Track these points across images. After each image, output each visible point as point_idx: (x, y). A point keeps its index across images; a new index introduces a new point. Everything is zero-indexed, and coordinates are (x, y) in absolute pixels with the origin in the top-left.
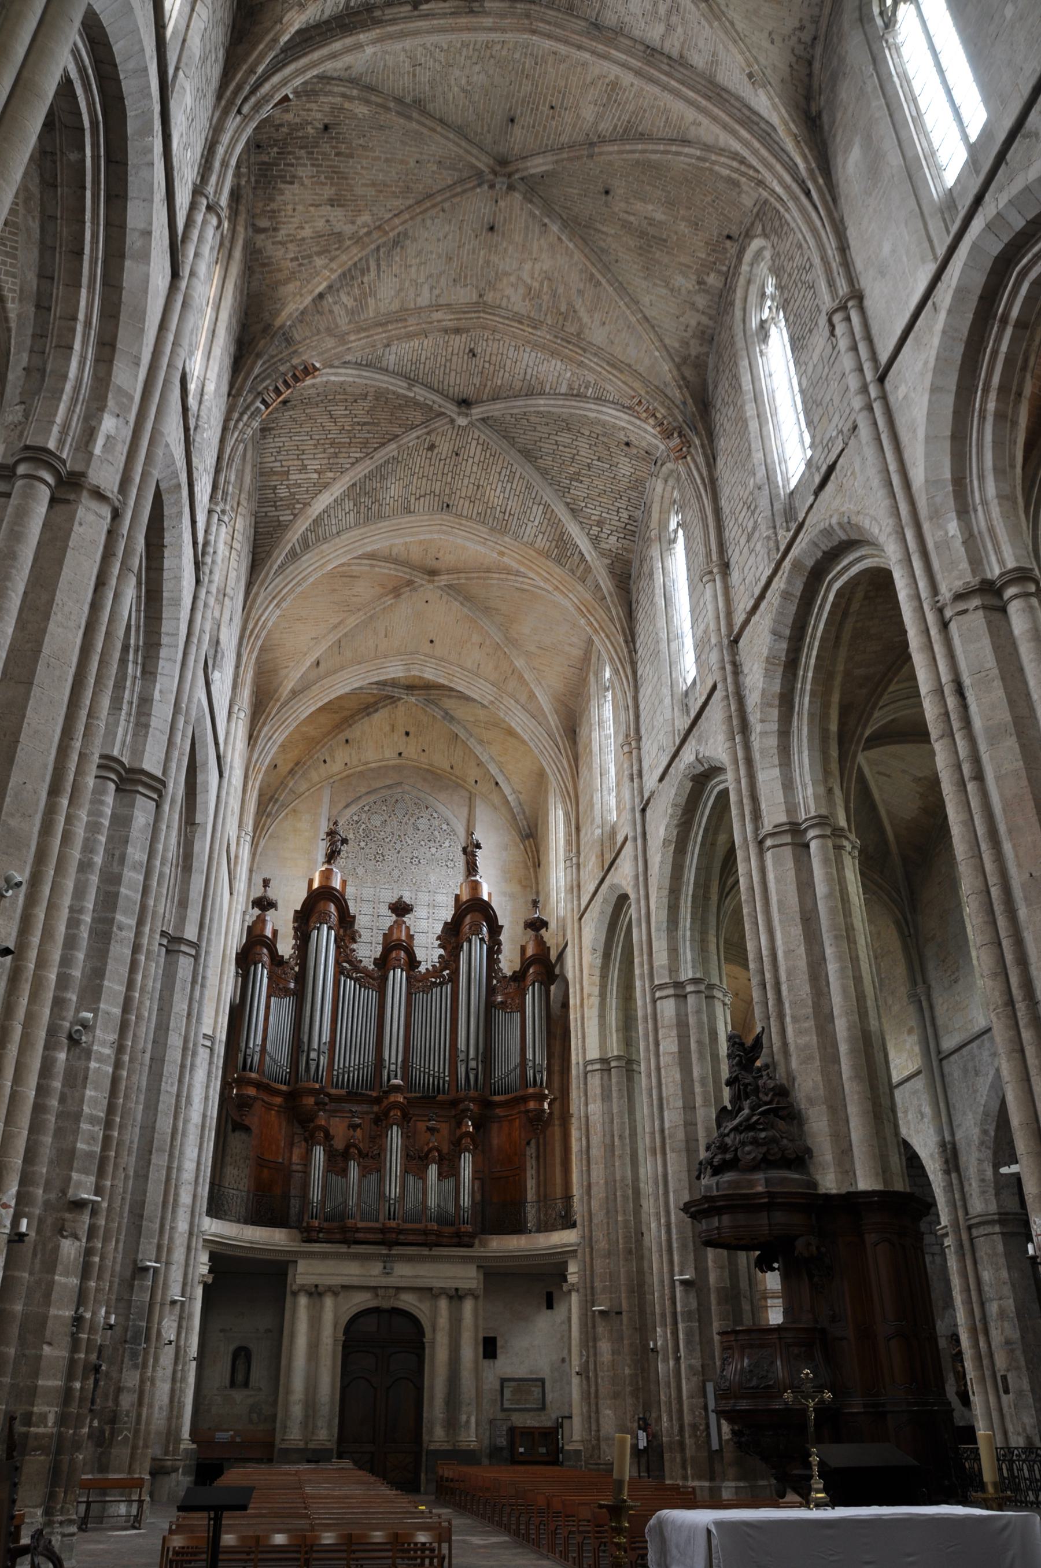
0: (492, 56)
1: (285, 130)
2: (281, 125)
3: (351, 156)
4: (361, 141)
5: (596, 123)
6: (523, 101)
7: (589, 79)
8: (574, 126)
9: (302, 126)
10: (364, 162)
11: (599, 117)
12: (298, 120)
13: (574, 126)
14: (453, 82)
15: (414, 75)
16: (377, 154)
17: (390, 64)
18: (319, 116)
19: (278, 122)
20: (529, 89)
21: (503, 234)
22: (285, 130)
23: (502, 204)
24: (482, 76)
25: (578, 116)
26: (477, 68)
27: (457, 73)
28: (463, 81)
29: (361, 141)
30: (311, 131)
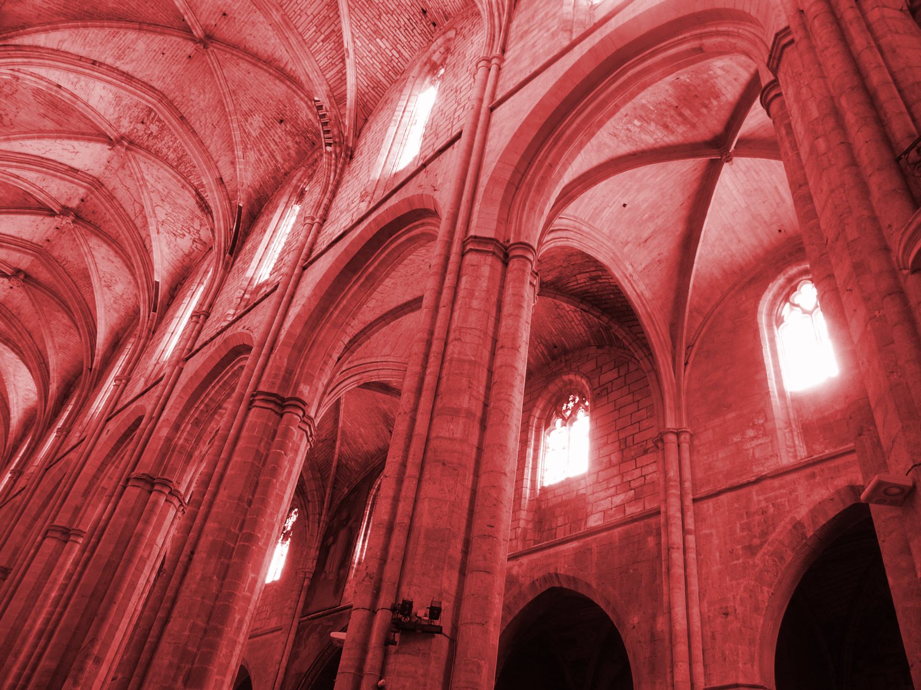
0: (184, 97)
1: (297, 139)
2: (296, 143)
3: (280, 100)
4: (271, 102)
5: (137, 39)
6: (179, 63)
7: (134, 64)
8: (152, 41)
9: (288, 133)
10: (275, 93)
11: (134, 42)
12: (289, 138)
13: (152, 41)
14: (206, 100)
15: (218, 122)
16: (267, 91)
17: (220, 142)
18: (279, 131)
19: (296, 146)
20: (174, 67)
21: (218, 8)
22: (297, 139)
23: (213, 23)
24: (193, 91)
25: (148, 45)
26: (192, 97)
27: (202, 104)
28: (202, 96)
29: (271, 102)
30: (288, 126)
